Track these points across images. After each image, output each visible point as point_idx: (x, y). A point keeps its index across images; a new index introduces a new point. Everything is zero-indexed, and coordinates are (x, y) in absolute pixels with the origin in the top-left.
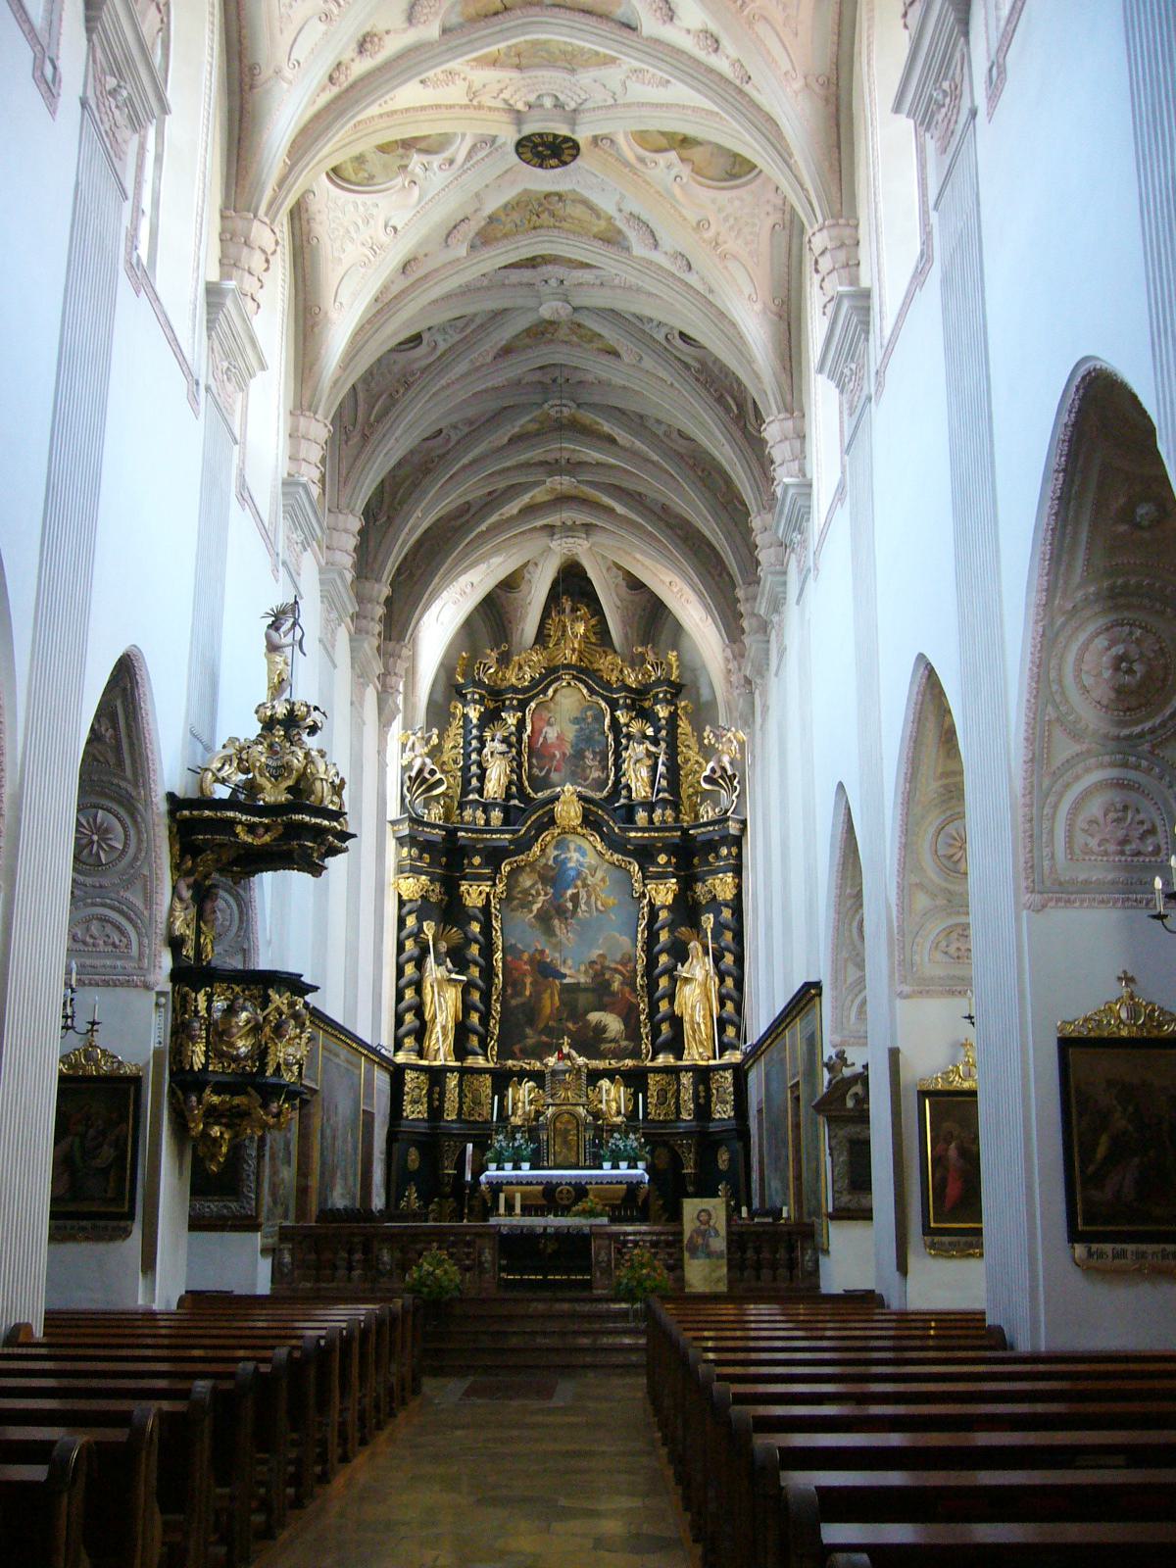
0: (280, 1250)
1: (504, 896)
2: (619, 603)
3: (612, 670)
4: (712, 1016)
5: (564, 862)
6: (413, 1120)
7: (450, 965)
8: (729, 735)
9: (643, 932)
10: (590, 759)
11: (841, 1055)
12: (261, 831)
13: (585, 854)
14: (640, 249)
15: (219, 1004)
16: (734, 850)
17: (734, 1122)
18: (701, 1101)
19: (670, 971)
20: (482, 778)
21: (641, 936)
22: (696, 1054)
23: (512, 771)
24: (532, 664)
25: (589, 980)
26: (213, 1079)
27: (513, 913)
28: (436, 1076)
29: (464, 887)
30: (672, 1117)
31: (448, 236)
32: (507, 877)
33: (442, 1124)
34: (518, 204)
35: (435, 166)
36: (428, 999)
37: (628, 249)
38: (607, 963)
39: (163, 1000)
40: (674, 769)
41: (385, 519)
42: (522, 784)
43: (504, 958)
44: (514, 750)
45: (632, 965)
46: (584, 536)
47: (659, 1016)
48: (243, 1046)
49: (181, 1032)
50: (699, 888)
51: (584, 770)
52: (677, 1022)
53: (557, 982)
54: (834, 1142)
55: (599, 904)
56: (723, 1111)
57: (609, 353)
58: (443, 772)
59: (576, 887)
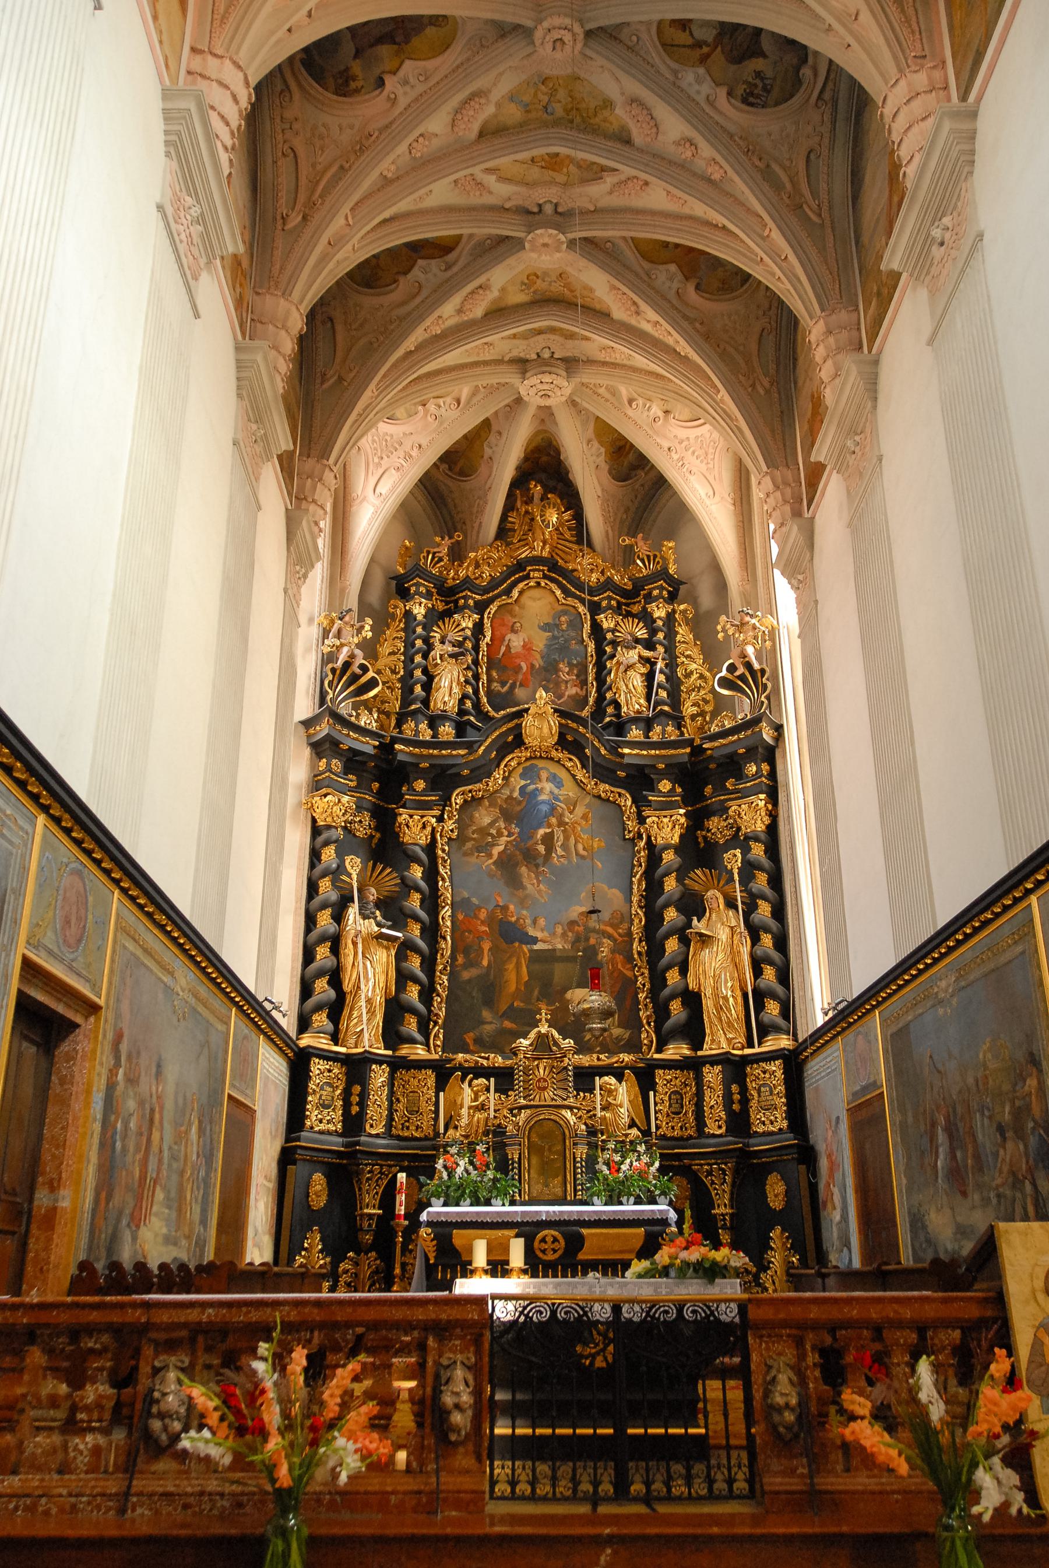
1: (454, 835)
2: (600, 494)
3: (592, 571)
5: (538, 791)
6: (321, 1132)
8: (754, 621)
9: (639, 884)
18: (736, 1107)
20: (428, 687)
21: (638, 886)
23: (467, 682)
25: (568, 946)
29: (403, 816)
30: (691, 1132)
32: (459, 811)
33: (363, 1139)
36: (348, 960)
41: (300, 218)
42: (478, 699)
44: (470, 659)
45: (626, 926)
46: (564, 374)
50: (714, 824)
51: (557, 684)
52: (692, 1000)
53: (525, 948)
55: (580, 847)
59: (549, 826)
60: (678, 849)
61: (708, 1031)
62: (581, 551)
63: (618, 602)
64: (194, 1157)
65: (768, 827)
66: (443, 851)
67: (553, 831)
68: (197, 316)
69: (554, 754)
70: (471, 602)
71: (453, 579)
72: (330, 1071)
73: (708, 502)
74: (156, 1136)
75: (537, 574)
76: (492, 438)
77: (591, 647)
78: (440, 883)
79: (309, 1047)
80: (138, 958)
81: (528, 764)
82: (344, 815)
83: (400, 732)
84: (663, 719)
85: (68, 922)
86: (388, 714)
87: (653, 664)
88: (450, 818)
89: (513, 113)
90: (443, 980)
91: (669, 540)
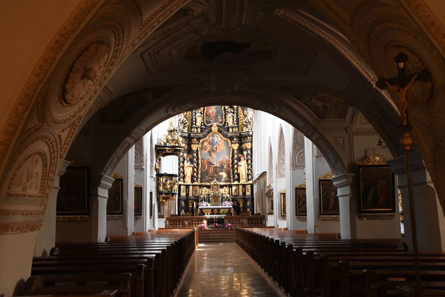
4: (246, 173)
6: (183, 196)
7: (190, 163)
9: (231, 155)
10: (219, 117)
11: (270, 185)
12: (170, 150)
13: (218, 138)
15: (164, 179)
16: (251, 138)
17: (251, 196)
18: (244, 191)
19: (237, 164)
20: (196, 122)
21: (231, 156)
22: (243, 181)
23: (202, 120)
25: (219, 166)
26: (164, 192)
27: (203, 151)
28: (187, 186)
29: (192, 146)
30: (238, 195)
38: (224, 162)
39: (155, 179)
40: (238, 119)
43: (201, 161)
44: (202, 115)
45: (229, 162)
48: (169, 187)
49: (158, 185)
50: (243, 145)
51: (218, 119)
52: (238, 175)
53: (213, 166)
54: (268, 201)
55: (221, 149)
56: (248, 193)
58: (187, 120)
59: (216, 145)
60: (237, 150)
61: (240, 180)
69: (217, 133)
77: (224, 112)
78: (199, 155)
83: (191, 131)
87: (234, 117)
90: (200, 171)
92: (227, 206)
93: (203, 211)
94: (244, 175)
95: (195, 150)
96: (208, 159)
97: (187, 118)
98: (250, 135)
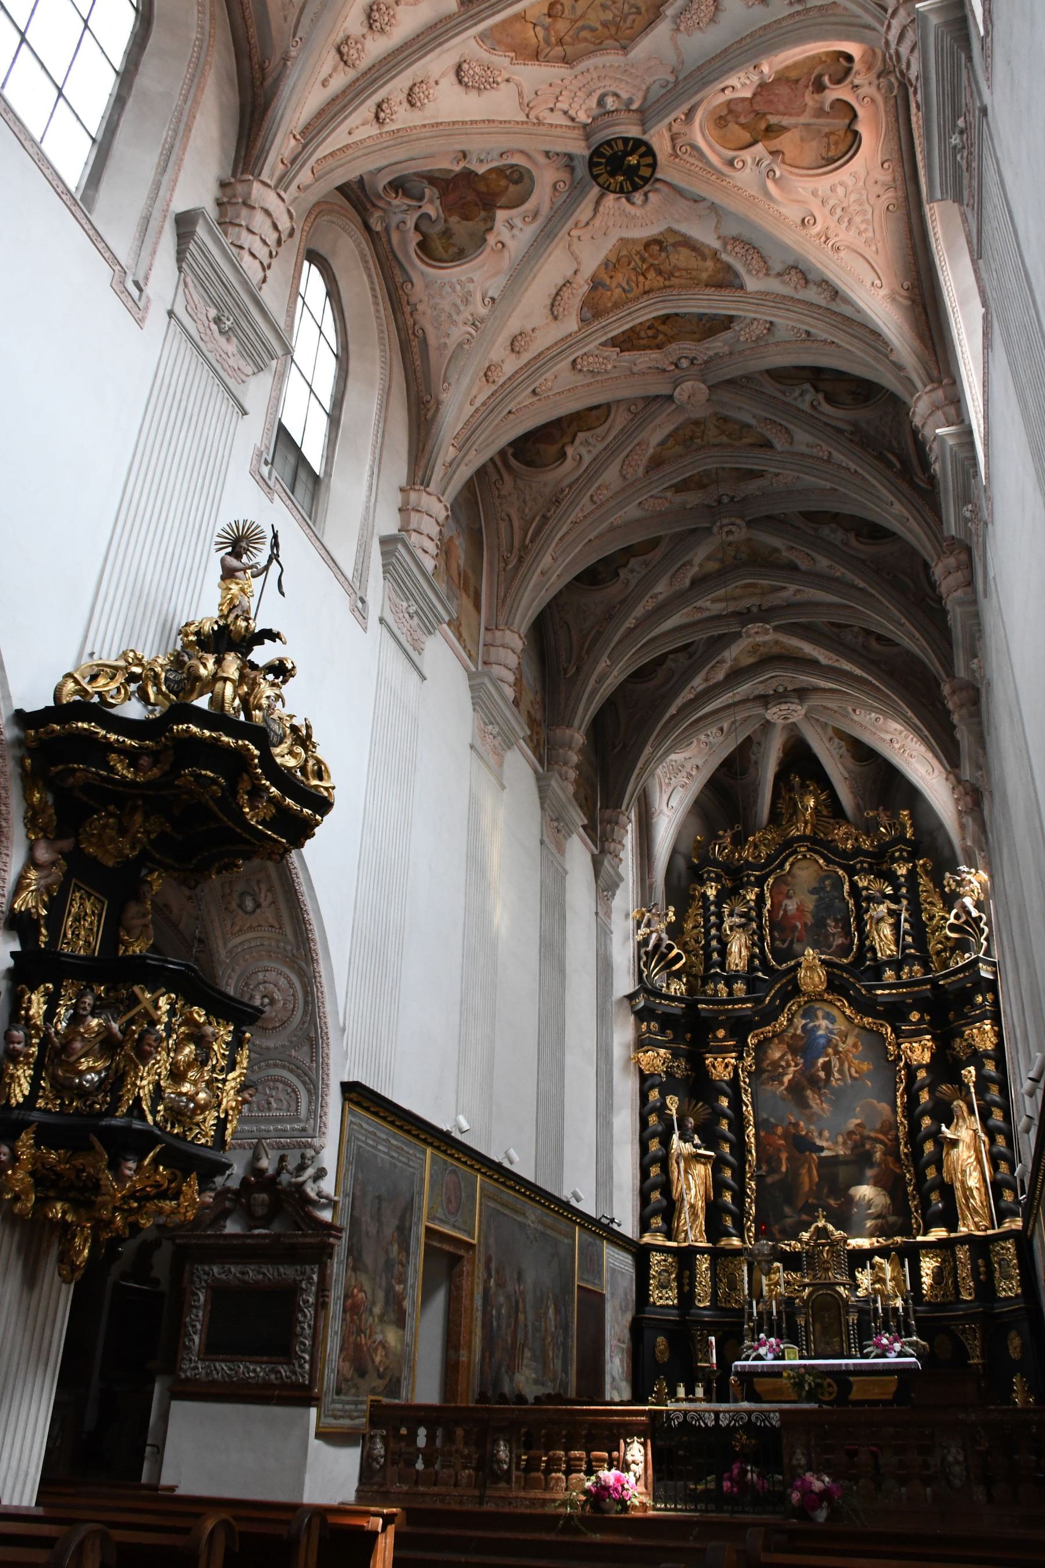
0: (372, 1437)
2: (847, 775)
3: (847, 839)
6: (661, 1306)
7: (697, 1141)
9: (902, 1096)
14: (752, 284)
16: (989, 996)
19: (935, 1135)
20: (724, 952)
23: (754, 944)
24: (766, 842)
25: (848, 1152)
27: (763, 1087)
28: (685, 1257)
31: (553, 305)
34: (618, 260)
35: (518, 222)
37: (742, 287)
38: (866, 1133)
41: (574, 670)
44: (754, 925)
45: (893, 1132)
46: (797, 701)
47: (927, 1185)
50: (958, 1043)
52: (947, 1191)
53: (814, 1156)
55: (853, 1070)
56: (1009, 1288)
57: (761, 446)
59: (827, 1055)
62: (837, 823)
63: (870, 864)
64: (553, 1329)
65: (997, 1045)
66: (745, 1083)
67: (830, 1061)
68: (503, 787)
70: (752, 878)
71: (739, 860)
72: (665, 1260)
73: (928, 777)
74: (521, 1317)
75: (802, 849)
76: (755, 748)
77: (851, 902)
78: (744, 1108)
79: (647, 1244)
80: (498, 1211)
81: (807, 1006)
82: (663, 1064)
83: (704, 993)
84: (910, 961)
85: (449, 1201)
86: (695, 976)
88: (748, 1056)
89: (713, 566)
91: (904, 810)
92: (892, 1359)
93: (758, 1388)
94: (976, 1193)
95: (722, 1080)
96: (790, 1123)
97: (686, 943)
98: (983, 984)
